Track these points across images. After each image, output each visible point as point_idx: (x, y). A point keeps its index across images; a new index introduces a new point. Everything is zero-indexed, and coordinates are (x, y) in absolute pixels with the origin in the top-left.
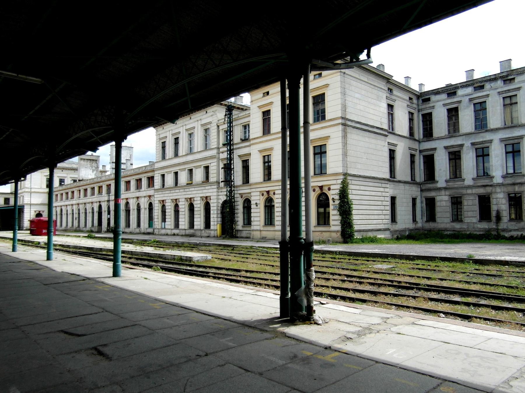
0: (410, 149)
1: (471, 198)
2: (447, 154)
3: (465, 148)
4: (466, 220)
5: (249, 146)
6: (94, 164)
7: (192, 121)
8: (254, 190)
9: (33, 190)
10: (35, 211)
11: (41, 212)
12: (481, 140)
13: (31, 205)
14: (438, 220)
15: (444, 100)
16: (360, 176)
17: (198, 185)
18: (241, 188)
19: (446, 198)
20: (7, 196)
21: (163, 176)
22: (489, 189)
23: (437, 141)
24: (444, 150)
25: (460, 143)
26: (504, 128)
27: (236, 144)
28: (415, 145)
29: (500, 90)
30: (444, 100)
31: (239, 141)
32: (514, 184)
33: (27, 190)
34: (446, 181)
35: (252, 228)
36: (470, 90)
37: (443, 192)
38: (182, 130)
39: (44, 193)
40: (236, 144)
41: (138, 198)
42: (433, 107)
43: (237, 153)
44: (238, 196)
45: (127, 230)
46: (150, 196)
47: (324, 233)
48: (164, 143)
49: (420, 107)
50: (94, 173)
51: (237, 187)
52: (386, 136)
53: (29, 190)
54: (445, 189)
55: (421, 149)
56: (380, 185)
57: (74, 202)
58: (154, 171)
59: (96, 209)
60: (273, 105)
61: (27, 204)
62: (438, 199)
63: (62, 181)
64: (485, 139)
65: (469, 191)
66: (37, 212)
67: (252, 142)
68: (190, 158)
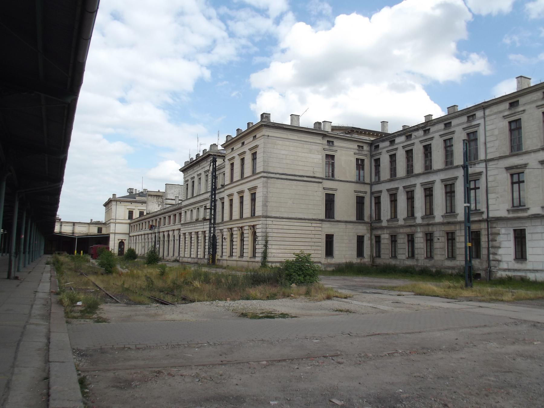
0: (355, 191)
1: (403, 237)
2: (389, 196)
3: (399, 190)
4: (399, 257)
5: (223, 191)
6: (160, 200)
7: (200, 168)
8: (225, 227)
9: (117, 221)
10: (119, 240)
11: (123, 241)
12: (409, 184)
13: (115, 233)
14: (382, 256)
15: (387, 147)
16: (283, 218)
17: (201, 221)
18: (221, 225)
19: (387, 236)
20: (99, 226)
21: (186, 212)
22: (413, 229)
23: (383, 184)
24: (387, 193)
25: (396, 186)
26: (424, 174)
27: (219, 189)
28: (367, 188)
29: (421, 139)
30: (387, 147)
31: (220, 187)
32: (428, 225)
33: (112, 221)
34: (388, 221)
35: (224, 258)
36: (403, 138)
37: (385, 231)
38: (195, 175)
39: (126, 223)
40: (219, 189)
41: (174, 230)
42: (380, 154)
43: (217, 197)
44: (219, 231)
45: (168, 258)
46: (179, 229)
47: (254, 263)
48: (187, 185)
49: (374, 153)
50: (161, 206)
51: (218, 224)
52: (321, 183)
53: (114, 221)
54: (387, 228)
55: (373, 191)
56: (310, 225)
57: (142, 233)
58: (180, 208)
59: (154, 239)
60: (235, 159)
61: (112, 233)
62: (383, 236)
63: (141, 213)
64: (412, 184)
65: (401, 230)
66: (120, 241)
67: (226, 188)
68: (198, 199)
